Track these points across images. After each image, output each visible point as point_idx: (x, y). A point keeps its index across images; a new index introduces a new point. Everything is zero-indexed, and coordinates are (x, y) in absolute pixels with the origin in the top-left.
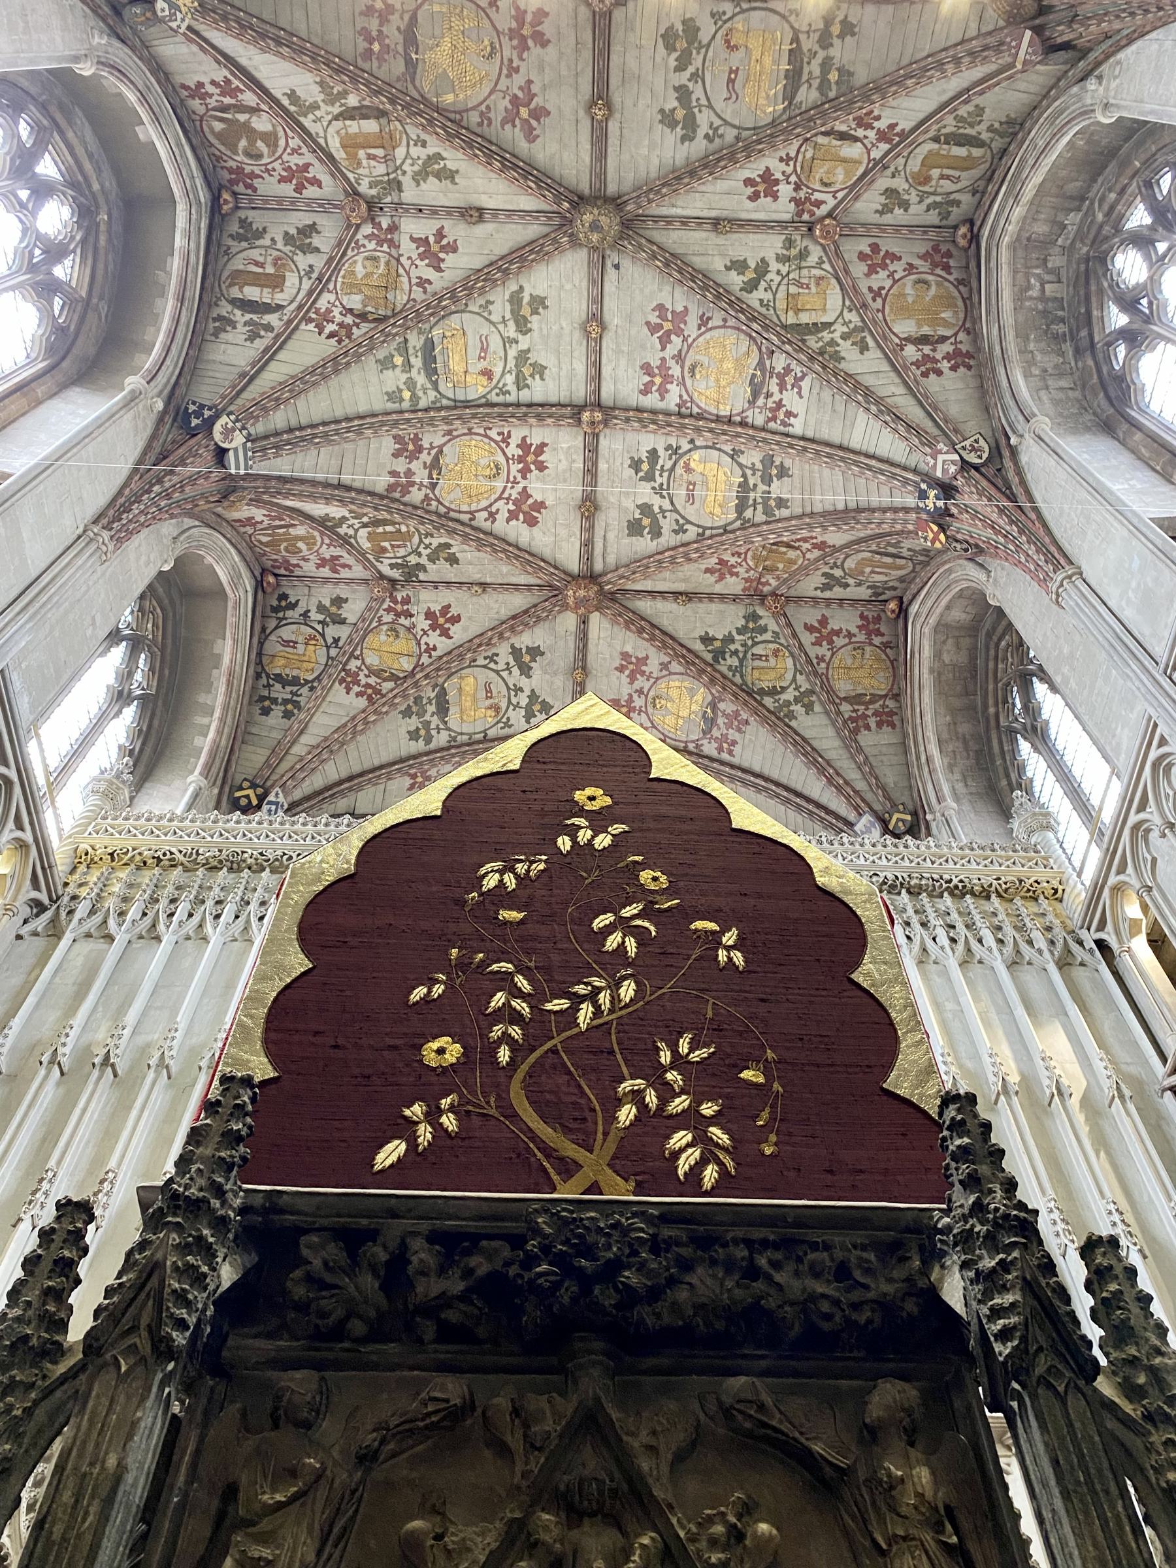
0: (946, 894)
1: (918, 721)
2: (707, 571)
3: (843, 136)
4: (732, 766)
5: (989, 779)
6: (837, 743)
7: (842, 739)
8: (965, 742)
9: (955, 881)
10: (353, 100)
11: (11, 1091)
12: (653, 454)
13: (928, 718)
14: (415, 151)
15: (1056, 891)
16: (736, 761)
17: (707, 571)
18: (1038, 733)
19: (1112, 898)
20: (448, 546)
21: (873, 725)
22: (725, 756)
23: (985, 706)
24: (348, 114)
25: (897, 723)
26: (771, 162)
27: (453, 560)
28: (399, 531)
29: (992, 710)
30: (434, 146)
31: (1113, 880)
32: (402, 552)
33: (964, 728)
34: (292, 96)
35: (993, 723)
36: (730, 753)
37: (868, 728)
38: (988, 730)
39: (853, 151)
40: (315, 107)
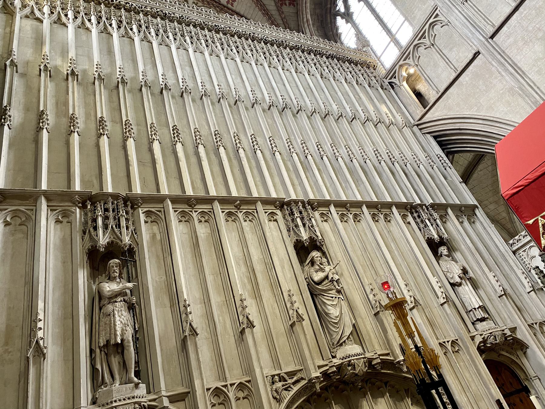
0: (346, 62)
1: (304, 5)
4: (232, 11)
5: (325, 31)
6: (275, 8)
7: (277, 7)
8: (318, 16)
9: (349, 58)
11: (27, 81)
13: (308, 5)
15: (374, 66)
16: (234, 8)
18: (348, 16)
19: (399, 68)
21: (287, 4)
22: (230, 6)
23: (326, 5)
25: (296, 5)
29: (329, 6)
31: (401, 62)
33: (318, 11)
35: (328, 11)
36: (232, 5)
37: (286, 5)
38: (326, 13)
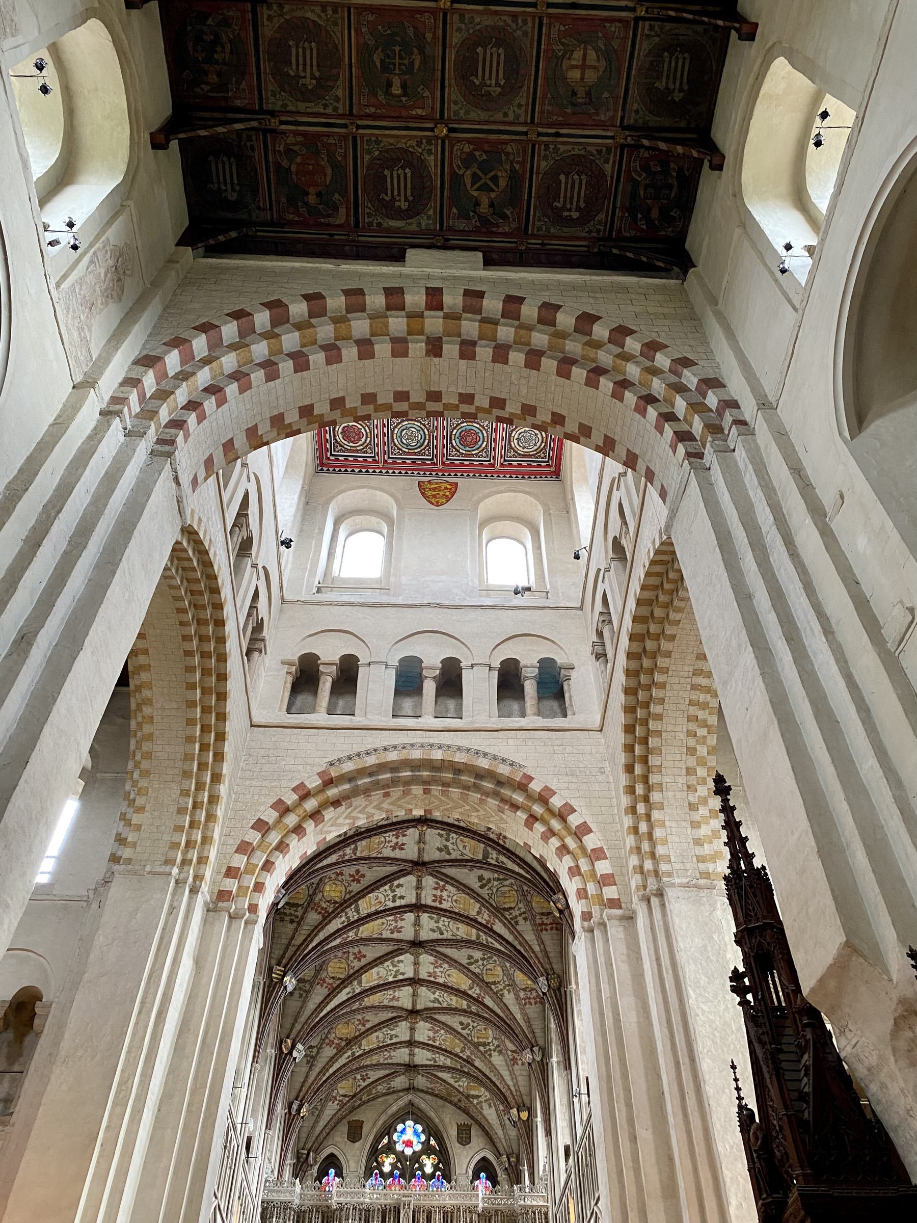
2: (369, 1021)
3: (345, 1096)
10: (475, 1101)
12: (391, 1039)
14: (461, 1084)
17: (369, 1021)
20: (463, 1029)
24: (478, 1097)
26: (364, 1084)
27: (461, 1023)
28: (478, 1038)
30: (456, 1085)
32: (479, 1028)
34: (490, 1106)
39: (342, 1092)
40: (486, 1101)
